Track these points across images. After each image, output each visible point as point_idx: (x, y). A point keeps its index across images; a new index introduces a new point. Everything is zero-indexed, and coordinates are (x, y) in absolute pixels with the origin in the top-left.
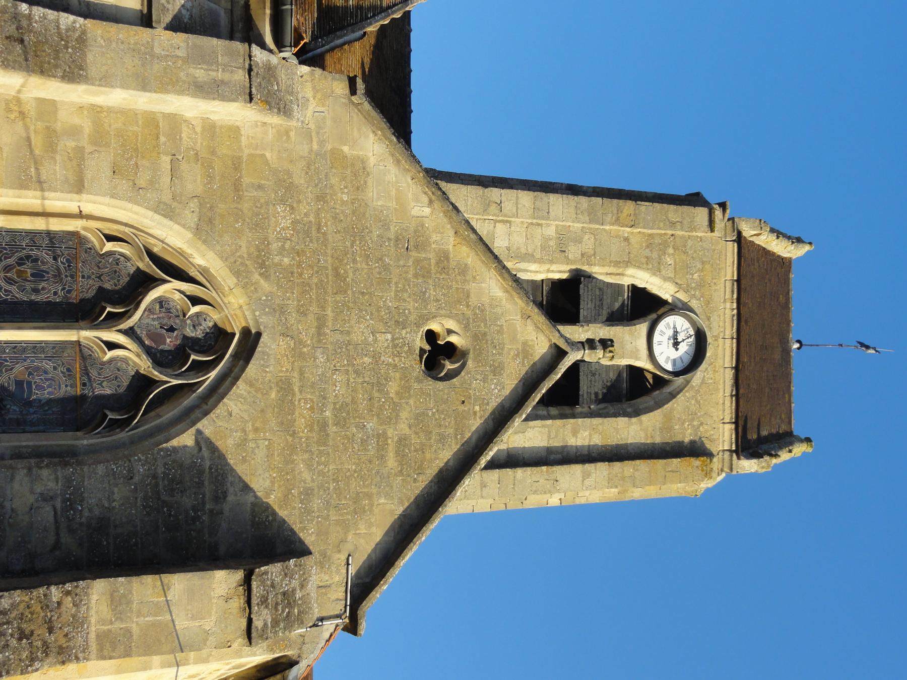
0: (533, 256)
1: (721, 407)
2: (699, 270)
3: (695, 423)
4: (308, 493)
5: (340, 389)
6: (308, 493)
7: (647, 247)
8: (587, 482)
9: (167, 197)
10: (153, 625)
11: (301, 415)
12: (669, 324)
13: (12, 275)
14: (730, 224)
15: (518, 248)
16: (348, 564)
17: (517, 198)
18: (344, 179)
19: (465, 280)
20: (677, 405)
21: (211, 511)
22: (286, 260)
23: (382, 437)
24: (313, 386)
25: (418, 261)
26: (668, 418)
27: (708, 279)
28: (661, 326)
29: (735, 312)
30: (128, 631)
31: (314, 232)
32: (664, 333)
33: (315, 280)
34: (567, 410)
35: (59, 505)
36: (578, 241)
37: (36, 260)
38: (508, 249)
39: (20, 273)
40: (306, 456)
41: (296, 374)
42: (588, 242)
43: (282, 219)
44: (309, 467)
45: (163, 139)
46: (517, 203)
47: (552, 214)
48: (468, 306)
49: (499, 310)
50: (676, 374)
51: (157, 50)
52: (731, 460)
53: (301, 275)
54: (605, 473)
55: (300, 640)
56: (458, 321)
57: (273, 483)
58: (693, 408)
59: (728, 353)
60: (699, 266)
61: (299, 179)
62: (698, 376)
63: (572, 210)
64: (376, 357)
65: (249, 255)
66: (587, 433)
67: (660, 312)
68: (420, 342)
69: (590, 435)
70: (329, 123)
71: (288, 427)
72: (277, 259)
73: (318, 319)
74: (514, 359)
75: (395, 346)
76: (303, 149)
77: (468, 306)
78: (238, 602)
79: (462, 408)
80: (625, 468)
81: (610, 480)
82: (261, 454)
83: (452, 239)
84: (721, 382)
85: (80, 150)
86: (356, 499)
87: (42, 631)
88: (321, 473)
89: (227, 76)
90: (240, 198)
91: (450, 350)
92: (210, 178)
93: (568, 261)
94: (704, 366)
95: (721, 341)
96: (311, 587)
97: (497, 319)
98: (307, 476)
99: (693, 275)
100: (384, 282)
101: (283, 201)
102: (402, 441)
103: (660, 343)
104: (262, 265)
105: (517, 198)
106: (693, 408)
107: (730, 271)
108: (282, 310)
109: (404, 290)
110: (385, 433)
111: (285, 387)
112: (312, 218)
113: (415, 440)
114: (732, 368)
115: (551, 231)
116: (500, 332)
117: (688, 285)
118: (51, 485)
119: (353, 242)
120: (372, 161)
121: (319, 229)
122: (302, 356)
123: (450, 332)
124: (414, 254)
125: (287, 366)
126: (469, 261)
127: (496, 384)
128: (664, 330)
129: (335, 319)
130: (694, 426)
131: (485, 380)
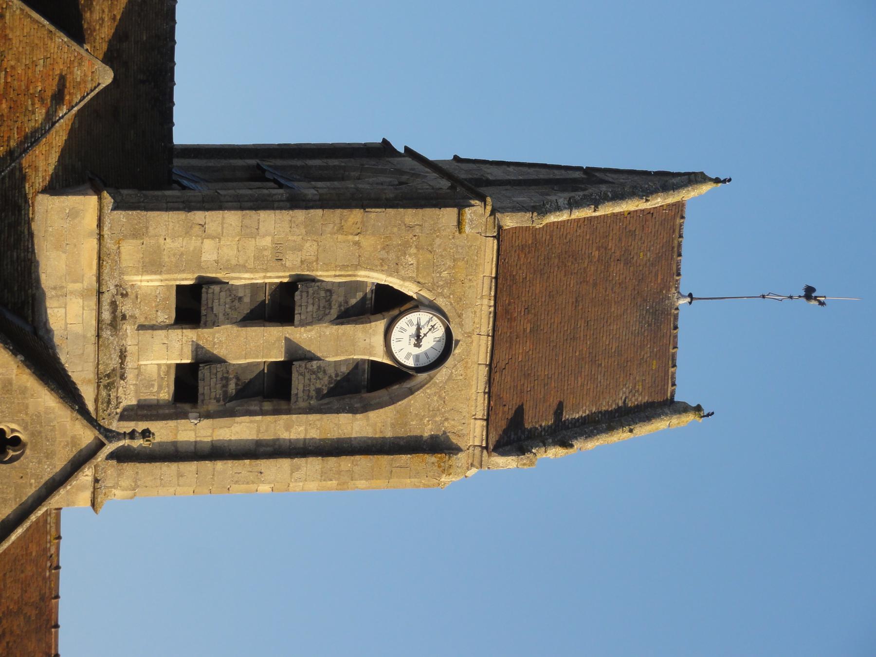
0: (244, 266)
1: (473, 403)
2: (449, 267)
3: (438, 419)
7: (384, 249)
8: (296, 475)
15: (228, 260)
17: (223, 218)
19: (25, 398)
20: (416, 403)
27: (461, 276)
28: (402, 323)
29: (492, 309)
32: (405, 330)
34: (283, 405)
38: (217, 262)
46: (223, 223)
47: (262, 230)
48: (27, 414)
49: (52, 416)
52: (481, 456)
54: (318, 467)
58: (436, 404)
59: (483, 350)
60: (449, 263)
62: (442, 374)
63: (286, 225)
66: (302, 428)
67: (403, 309)
69: (306, 430)
74: (63, 448)
77: (27, 414)
79: (21, 481)
80: (342, 463)
81: (323, 473)
83: (15, 371)
84: (474, 378)
93: (284, 268)
99: (440, 273)
103: (399, 340)
105: (223, 218)
107: (488, 268)
114: (486, 365)
115: (267, 242)
116: (53, 429)
117: (433, 284)
123: (13, 431)
126: (29, 385)
127: (49, 466)
128: (405, 327)
130: (436, 422)
131: (39, 462)
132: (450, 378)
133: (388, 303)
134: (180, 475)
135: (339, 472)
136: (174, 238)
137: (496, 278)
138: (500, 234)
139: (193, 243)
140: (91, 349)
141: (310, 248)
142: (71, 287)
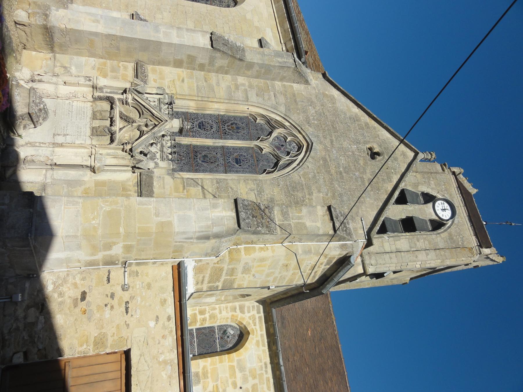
4: (341, 195)
5: (343, 162)
6: (341, 195)
9: (274, 103)
10: (298, 223)
11: (332, 169)
12: (439, 205)
13: (230, 127)
14: (449, 170)
16: (362, 220)
18: (328, 100)
21: (309, 198)
22: (316, 122)
24: (334, 160)
25: (358, 125)
26: (450, 234)
30: (290, 224)
31: (322, 114)
33: (326, 128)
35: (256, 192)
37: (236, 124)
39: (232, 127)
40: (337, 182)
41: (327, 156)
43: (312, 111)
44: (339, 186)
45: (270, 88)
51: (265, 53)
53: (322, 127)
55: (351, 246)
56: (378, 144)
57: (328, 191)
58: (458, 231)
64: (353, 152)
65: (304, 120)
66: (422, 241)
70: (320, 85)
72: (313, 122)
73: (331, 140)
75: (358, 150)
76: (314, 92)
78: (328, 217)
79: (387, 170)
82: (321, 181)
85: (246, 90)
87: (260, 217)
88: (344, 188)
89: (288, 61)
90: (297, 104)
92: (287, 99)
94: (456, 216)
95: (460, 208)
97: (390, 144)
98: (339, 189)
101: (311, 105)
104: (308, 123)
106: (458, 231)
108: (318, 136)
109: (356, 133)
110: (363, 177)
111: (325, 160)
112: (321, 111)
118: (252, 186)
119: (336, 118)
120: (336, 96)
121: (324, 114)
122: (328, 150)
124: (356, 122)
125: (324, 153)
129: (336, 140)
135: (441, 255)
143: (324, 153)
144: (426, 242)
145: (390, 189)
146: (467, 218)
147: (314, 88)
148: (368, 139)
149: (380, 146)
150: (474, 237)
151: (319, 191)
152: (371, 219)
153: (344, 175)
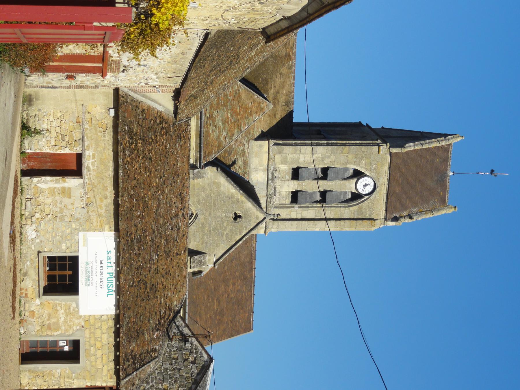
4: (207, 243)
6: (207, 243)
23: (223, 233)
26: (360, 208)
27: (379, 167)
28: (361, 180)
36: (329, 157)
42: (333, 158)
44: (207, 238)
47: (318, 152)
50: (366, 195)
61: (206, 187)
62: (373, 196)
63: (325, 150)
64: (222, 219)
68: (232, 215)
71: (203, 231)
76: (208, 181)
82: (198, 236)
86: (217, 244)
91: (240, 217)
93: (325, 164)
96: (207, 259)
98: (207, 240)
100: (224, 205)
102: (227, 234)
103: (360, 186)
107: (387, 165)
113: (230, 234)
115: (320, 155)
116: (251, 213)
120: (222, 182)
132: (375, 197)
133: (358, 174)
134: (292, 225)
135: (340, 225)
136: (291, 154)
137: (390, 168)
138: (391, 154)
139: (297, 156)
140: (265, 187)
141: (333, 158)
142: (260, 168)
143: (203, 220)
144: (333, 213)
145: (238, 238)
146: (385, 195)
147: (209, 179)
148: (235, 209)
149: (243, 213)
150: (384, 212)
151: (195, 241)
152: (220, 255)
153: (212, 231)
